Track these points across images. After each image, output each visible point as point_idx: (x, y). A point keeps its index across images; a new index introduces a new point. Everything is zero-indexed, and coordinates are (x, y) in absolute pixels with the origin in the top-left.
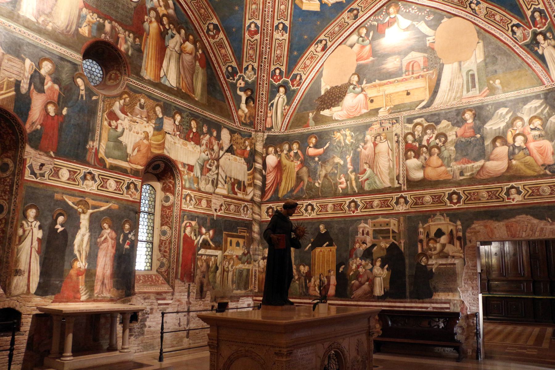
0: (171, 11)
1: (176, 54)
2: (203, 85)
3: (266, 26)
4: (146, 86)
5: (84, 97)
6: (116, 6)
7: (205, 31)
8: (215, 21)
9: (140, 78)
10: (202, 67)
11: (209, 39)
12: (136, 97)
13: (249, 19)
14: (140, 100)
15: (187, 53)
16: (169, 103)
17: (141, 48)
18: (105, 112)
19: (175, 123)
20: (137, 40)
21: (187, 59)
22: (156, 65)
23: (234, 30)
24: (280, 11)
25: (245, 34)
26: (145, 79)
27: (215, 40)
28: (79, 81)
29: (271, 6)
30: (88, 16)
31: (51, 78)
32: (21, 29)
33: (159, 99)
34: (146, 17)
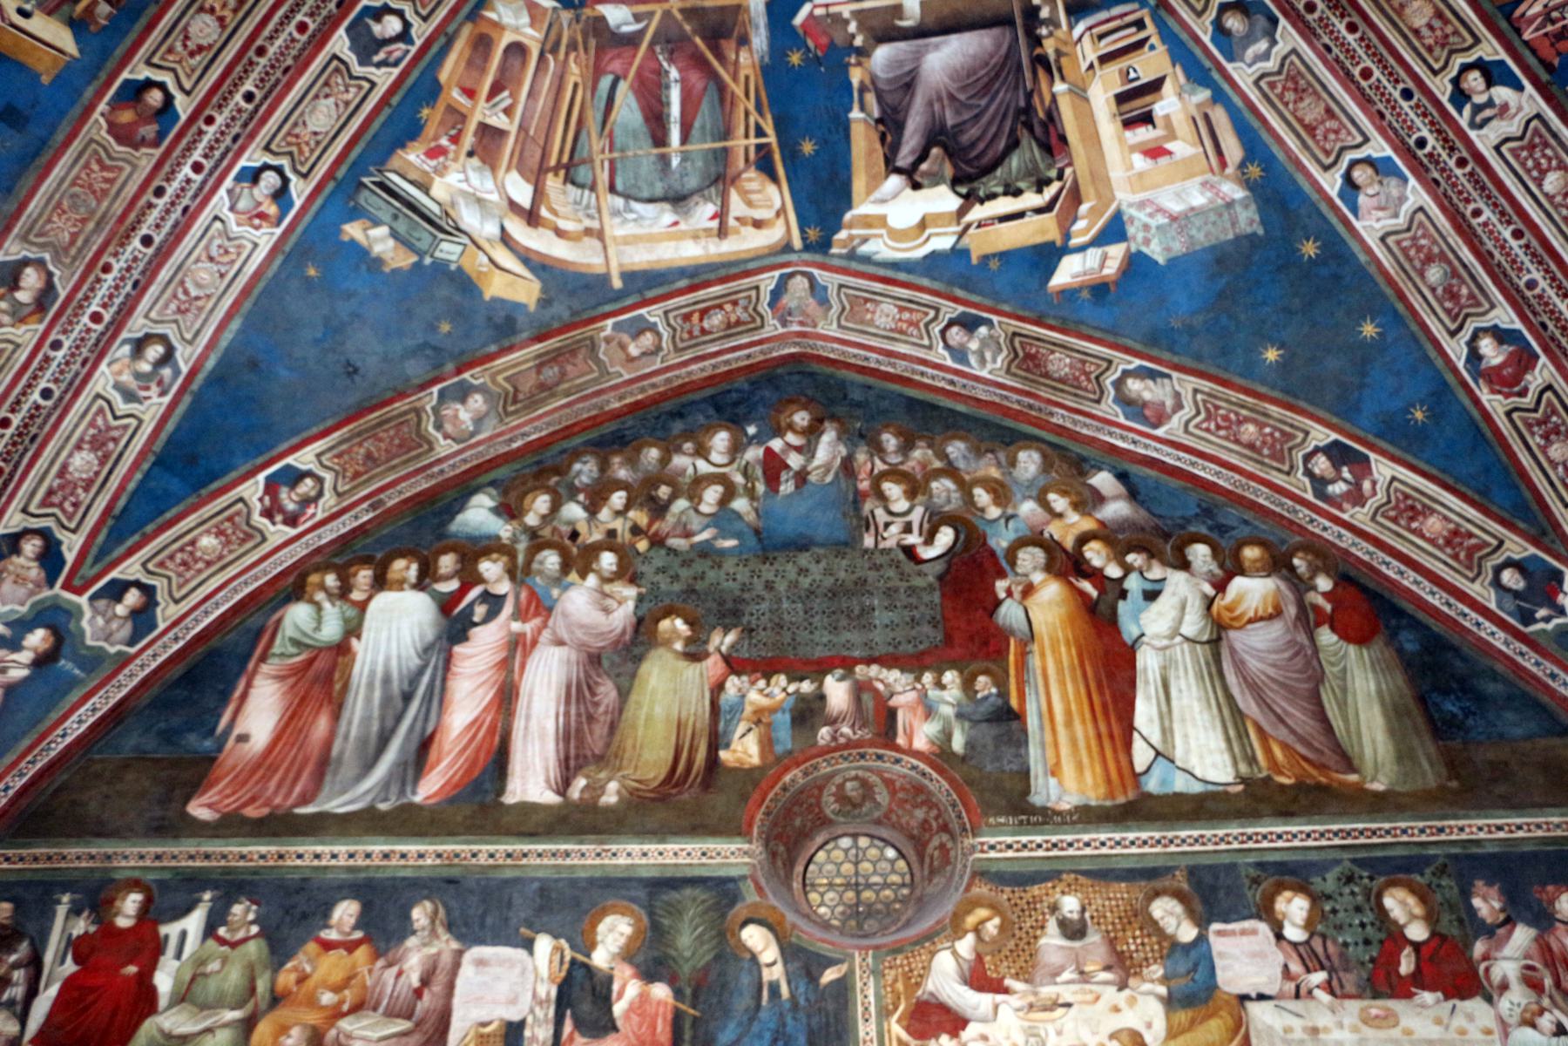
0: (1117, 509)
1: (1193, 652)
2: (1395, 714)
3: (1539, 309)
4: (1069, 838)
5: (785, 990)
6: (856, 612)
7: (1310, 496)
8: (1322, 435)
9: (1034, 819)
10: (1361, 640)
11: (1345, 517)
12: (1035, 900)
13: (1453, 334)
14: (1054, 908)
15: (1250, 621)
16: (1226, 859)
17: (1007, 703)
18: (889, 1014)
19: (1279, 936)
20: (982, 680)
21: (1260, 646)
22: (1099, 736)
23: (1419, 415)
24: (1556, 207)
25: (1477, 402)
26: (1059, 813)
27: (1371, 504)
28: (754, 937)
29: (1494, 219)
30: (753, 696)
31: (637, 966)
32: (510, 848)
33: (1159, 863)
34: (1001, 586)
